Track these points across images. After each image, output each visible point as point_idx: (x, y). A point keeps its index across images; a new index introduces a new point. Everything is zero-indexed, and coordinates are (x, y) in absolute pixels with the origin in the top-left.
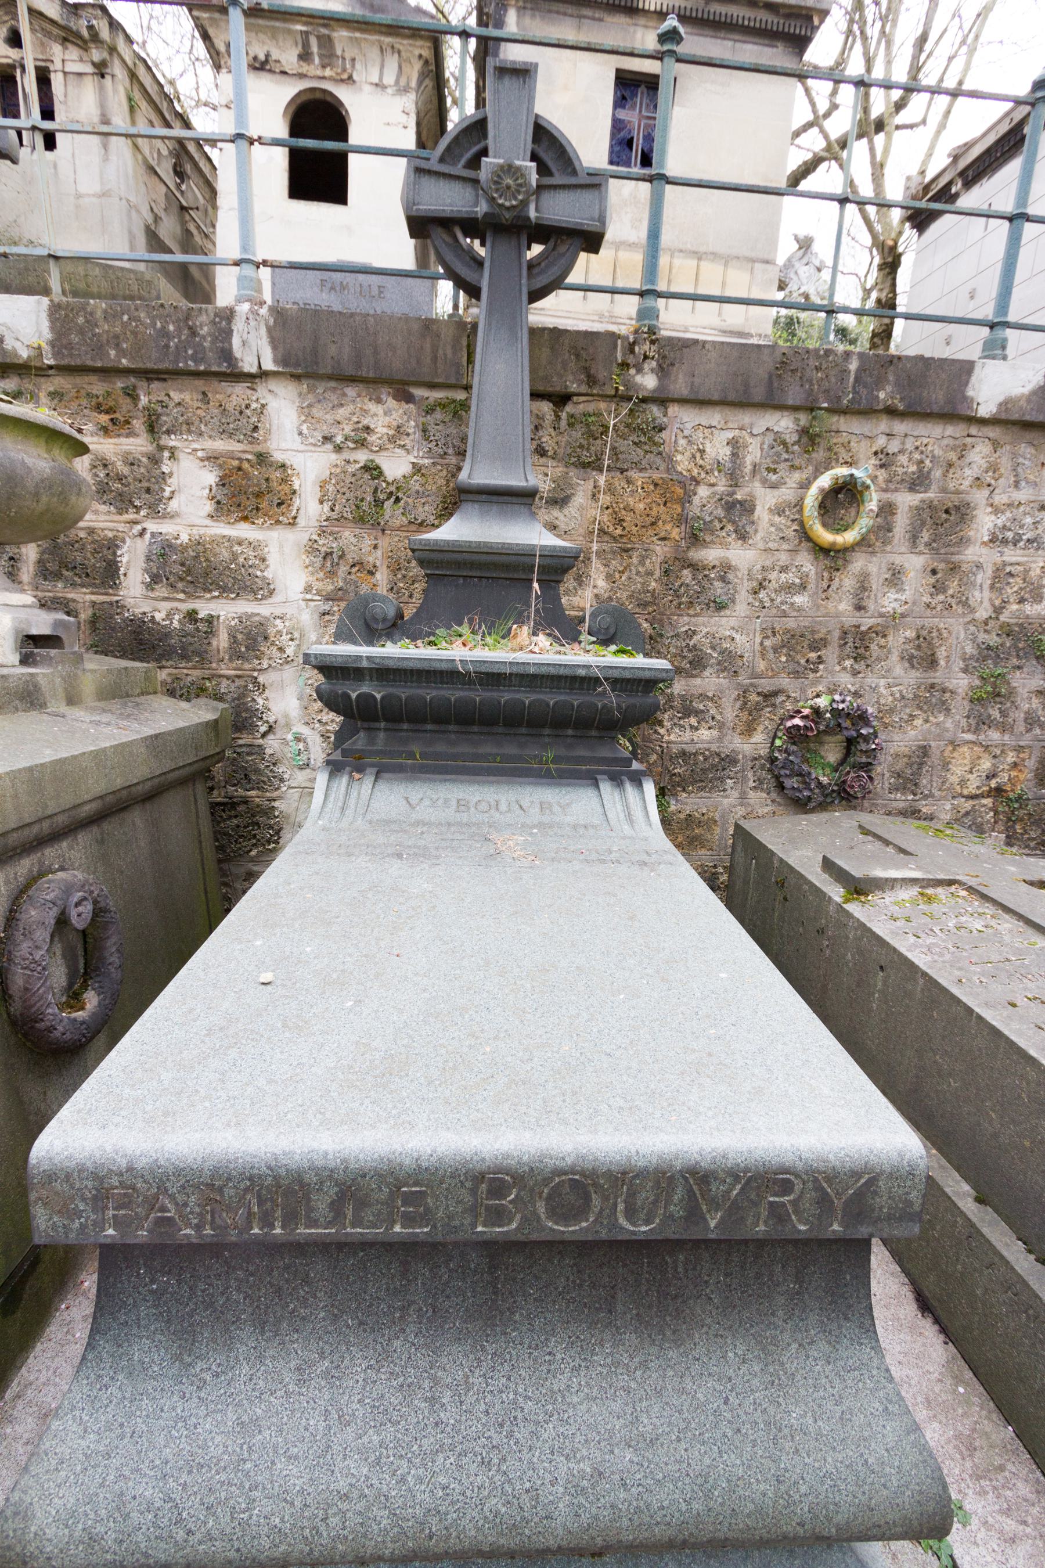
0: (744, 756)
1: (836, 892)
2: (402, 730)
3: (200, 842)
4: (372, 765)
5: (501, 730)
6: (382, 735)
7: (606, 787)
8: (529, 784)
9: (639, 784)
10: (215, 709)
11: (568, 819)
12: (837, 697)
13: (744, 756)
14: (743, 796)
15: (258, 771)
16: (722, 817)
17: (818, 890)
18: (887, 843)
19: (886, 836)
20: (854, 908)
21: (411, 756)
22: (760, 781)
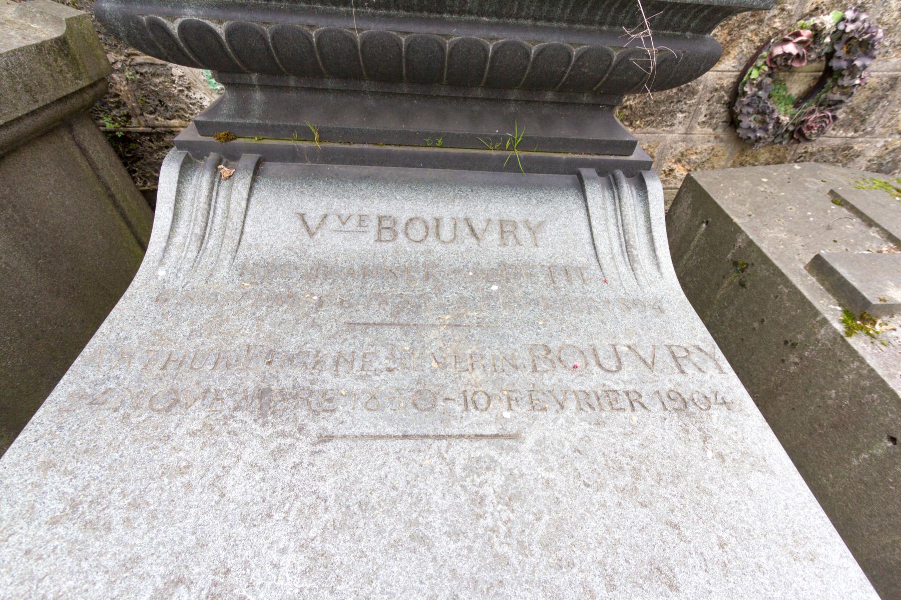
0: (705, 87)
1: (832, 312)
2: (287, 88)
3: (112, 196)
4: (250, 150)
5: (444, 92)
6: (258, 96)
7: (596, 193)
8: (484, 185)
9: (641, 186)
10: (56, 20)
11: (542, 254)
12: (849, 15)
13: (705, 87)
14: (689, 131)
15: (171, 96)
16: (661, 153)
17: (803, 300)
18: (870, 223)
19: (868, 212)
20: (858, 343)
21: (306, 135)
22: (711, 116)
